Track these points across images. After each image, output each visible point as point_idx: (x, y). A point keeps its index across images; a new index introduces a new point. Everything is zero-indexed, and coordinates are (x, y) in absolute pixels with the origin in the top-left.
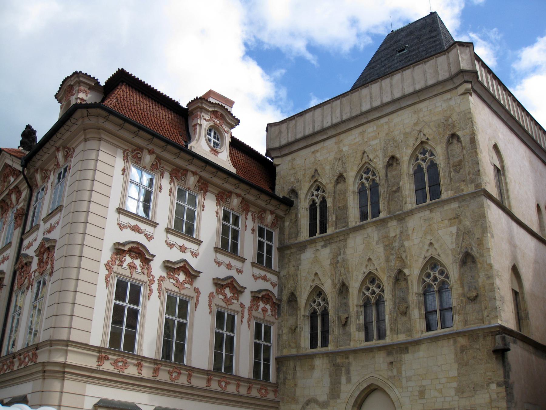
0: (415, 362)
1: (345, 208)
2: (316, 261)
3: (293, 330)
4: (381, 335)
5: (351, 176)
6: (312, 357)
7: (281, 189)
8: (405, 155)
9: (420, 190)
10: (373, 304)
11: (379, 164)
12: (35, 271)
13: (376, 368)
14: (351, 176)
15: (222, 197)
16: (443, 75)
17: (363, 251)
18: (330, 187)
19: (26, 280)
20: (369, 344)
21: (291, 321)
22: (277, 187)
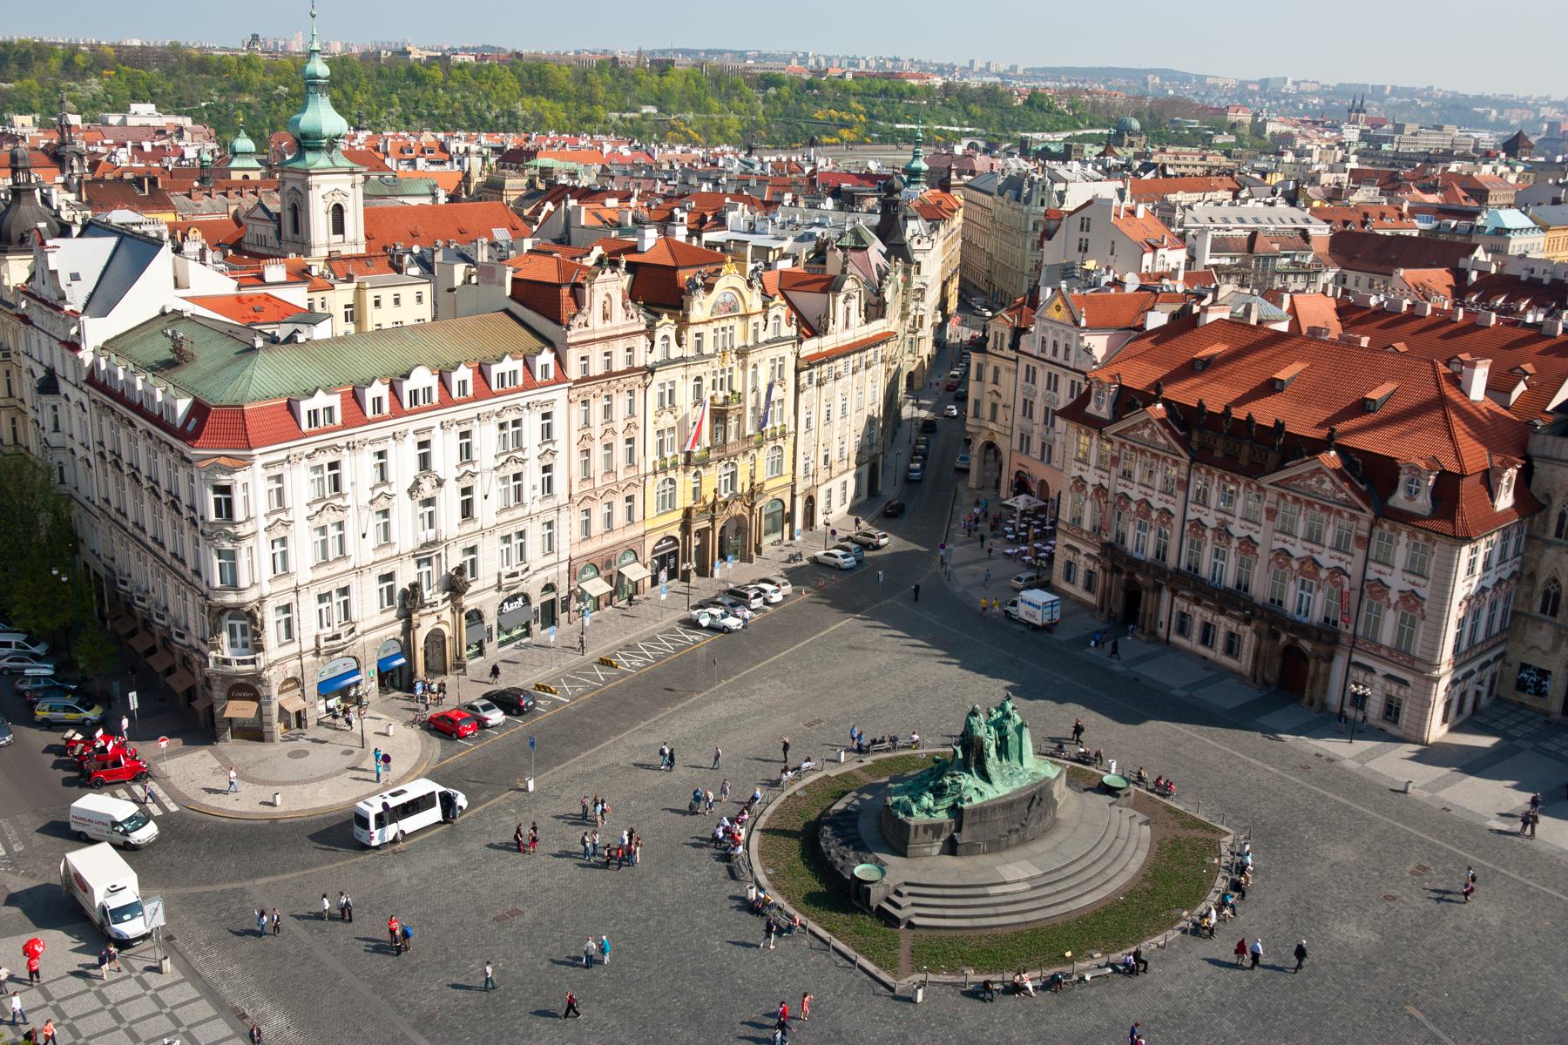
3: (1529, 596)
6: (1542, 621)
22: (1533, 486)
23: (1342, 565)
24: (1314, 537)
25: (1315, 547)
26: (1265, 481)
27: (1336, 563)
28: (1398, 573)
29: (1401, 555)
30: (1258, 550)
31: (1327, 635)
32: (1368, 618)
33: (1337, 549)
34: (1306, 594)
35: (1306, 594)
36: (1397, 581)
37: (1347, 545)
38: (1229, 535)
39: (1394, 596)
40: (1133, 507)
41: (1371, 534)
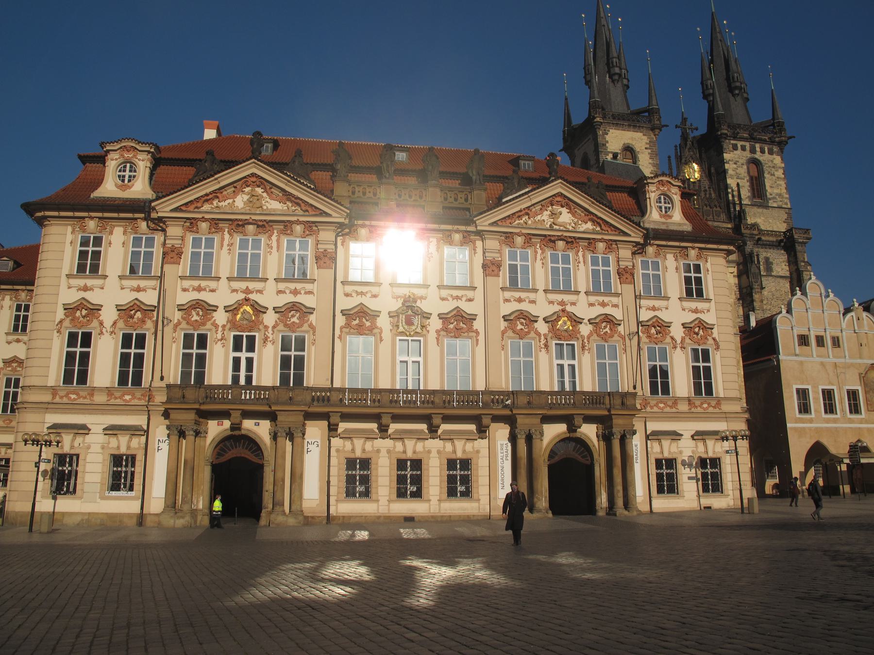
12: (683, 339)
19: (668, 340)
23: (608, 310)
24: (561, 284)
25: (567, 298)
26: (484, 223)
27: (598, 311)
29: (673, 282)
30: (478, 325)
31: (610, 411)
33: (596, 292)
34: (566, 363)
35: (566, 363)
37: (608, 285)
38: (427, 316)
39: (677, 332)
40: (221, 317)
41: (633, 266)
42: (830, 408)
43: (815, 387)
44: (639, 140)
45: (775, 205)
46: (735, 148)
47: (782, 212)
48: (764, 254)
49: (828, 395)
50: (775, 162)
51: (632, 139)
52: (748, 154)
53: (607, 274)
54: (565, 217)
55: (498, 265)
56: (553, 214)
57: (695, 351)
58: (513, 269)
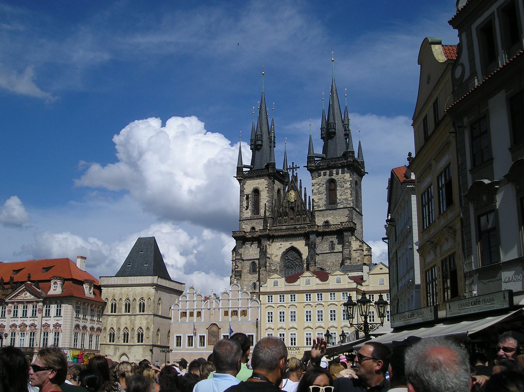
0: (134, 349)
1: (121, 308)
2: (112, 321)
4: (127, 342)
5: (124, 300)
7: (103, 297)
8: (138, 299)
9: (140, 309)
10: (126, 336)
11: (131, 299)
13: (125, 349)
14: (124, 300)
15: (92, 306)
16: (149, 282)
17: (125, 321)
18: (118, 301)
20: (124, 344)
21: (104, 335)
27: (32, 322)
28: (52, 318)
30: (5, 328)
32: (44, 339)
35: (22, 338)
36: (52, 321)
39: (52, 327)
42: (190, 344)
43: (184, 335)
44: (262, 184)
45: (342, 206)
46: (319, 175)
47: (346, 210)
48: (331, 240)
49: (190, 338)
50: (345, 178)
51: (258, 184)
52: (327, 177)
53: (36, 310)
54: (28, 294)
55: (11, 312)
56: (25, 295)
57: (56, 333)
58: (14, 311)
